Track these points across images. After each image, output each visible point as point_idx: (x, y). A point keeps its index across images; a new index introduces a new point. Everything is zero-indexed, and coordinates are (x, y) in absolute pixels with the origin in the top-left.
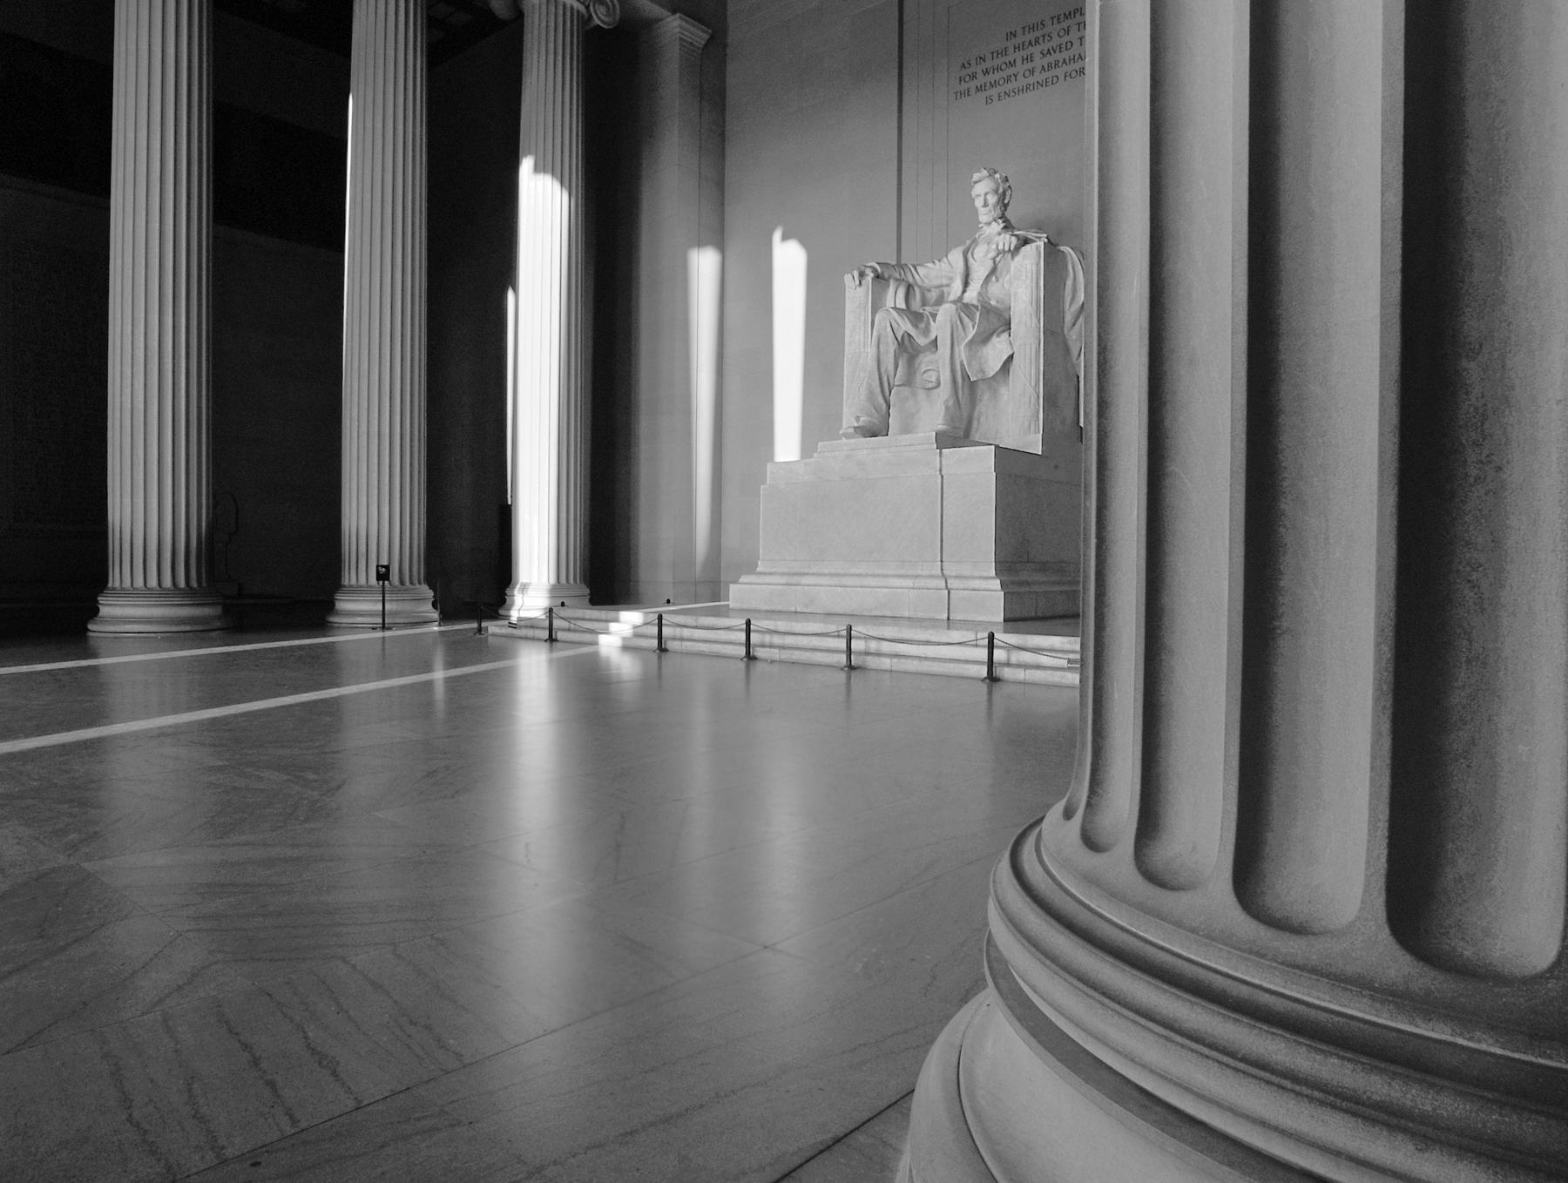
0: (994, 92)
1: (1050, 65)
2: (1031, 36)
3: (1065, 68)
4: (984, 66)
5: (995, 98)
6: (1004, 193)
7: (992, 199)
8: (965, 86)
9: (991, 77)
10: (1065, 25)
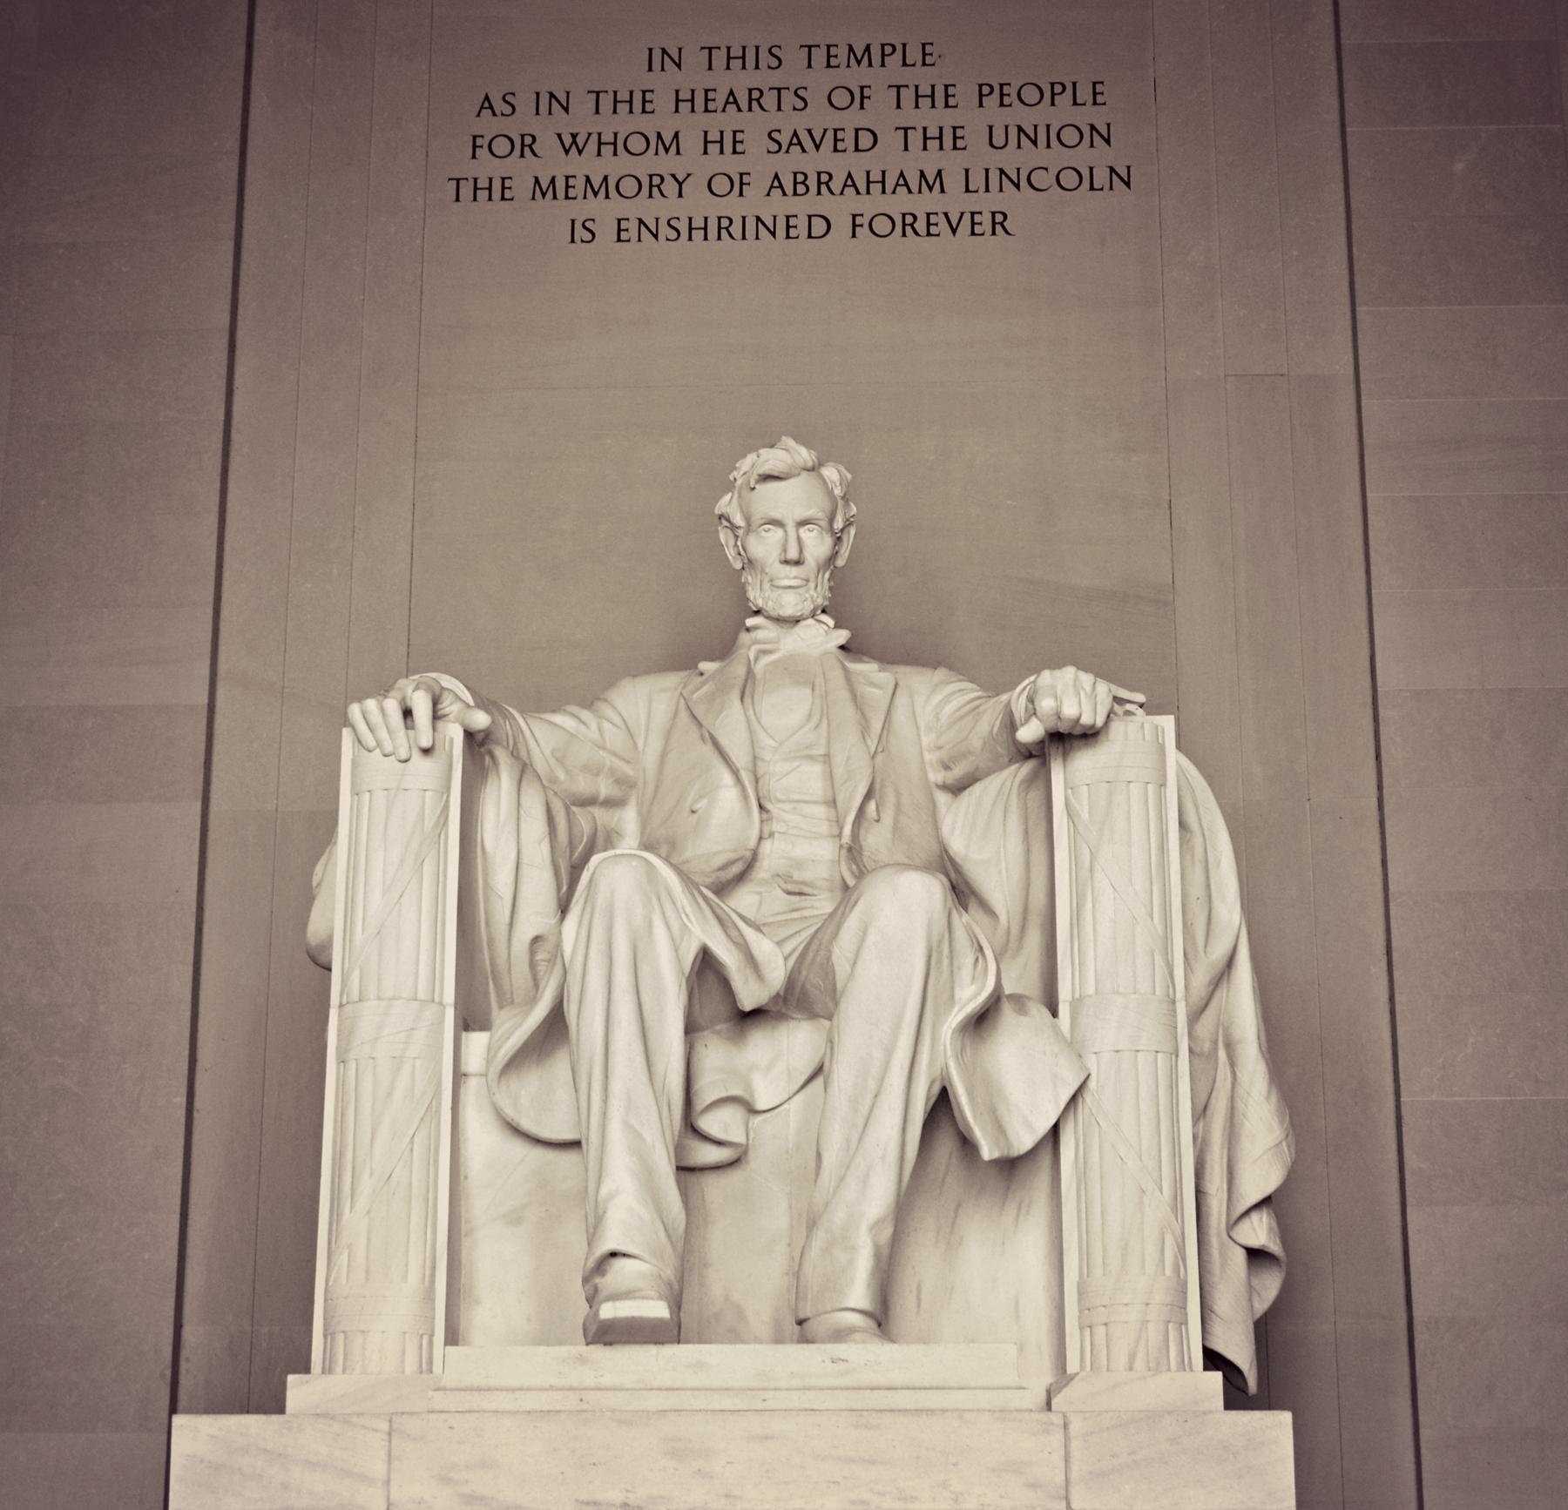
0: (604, 211)
1: (799, 179)
2: (741, 81)
3: (851, 202)
4: (562, 123)
5: (606, 230)
6: (839, 539)
7: (816, 545)
8: (486, 167)
9: (588, 165)
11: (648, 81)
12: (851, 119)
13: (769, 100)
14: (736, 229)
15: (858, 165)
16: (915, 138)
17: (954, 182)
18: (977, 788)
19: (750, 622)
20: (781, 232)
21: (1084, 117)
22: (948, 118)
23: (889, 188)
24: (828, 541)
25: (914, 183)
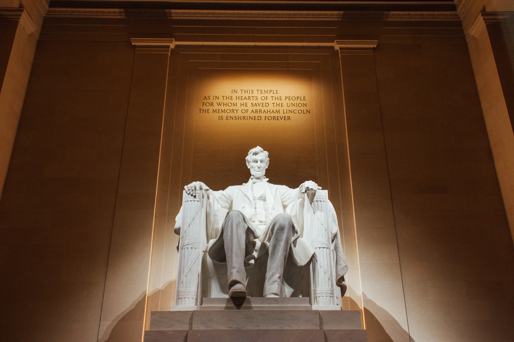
0: (224, 115)
1: (256, 111)
2: (247, 95)
3: (265, 114)
5: (225, 118)
8: (205, 108)
10: (265, 95)
11: (232, 95)
12: (265, 101)
13: (251, 98)
14: (246, 118)
15: (266, 109)
16: (275, 105)
17: (281, 112)
18: (292, 204)
19: (252, 177)
20: (253, 118)
21: (302, 102)
22: (280, 102)
23: (271, 112)
24: (265, 164)
25: (275, 111)
